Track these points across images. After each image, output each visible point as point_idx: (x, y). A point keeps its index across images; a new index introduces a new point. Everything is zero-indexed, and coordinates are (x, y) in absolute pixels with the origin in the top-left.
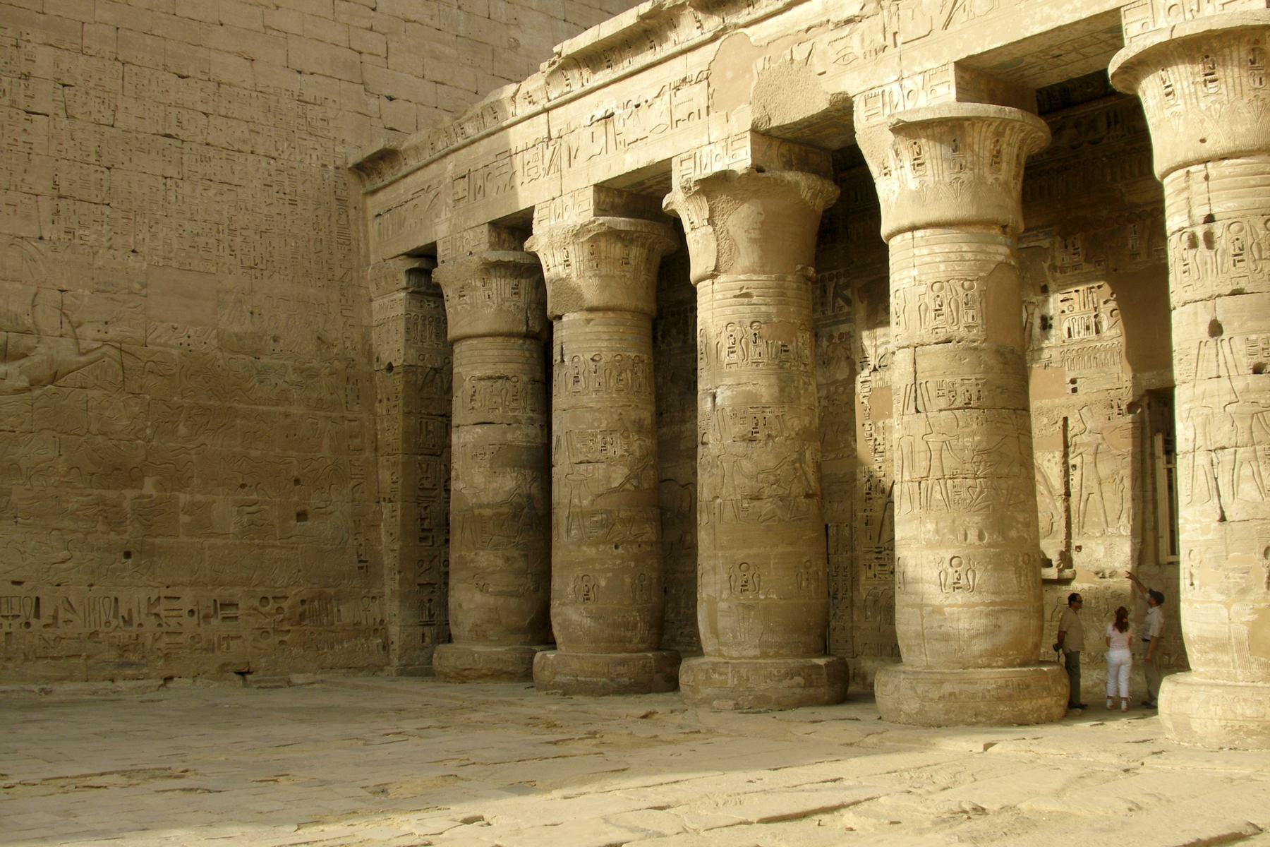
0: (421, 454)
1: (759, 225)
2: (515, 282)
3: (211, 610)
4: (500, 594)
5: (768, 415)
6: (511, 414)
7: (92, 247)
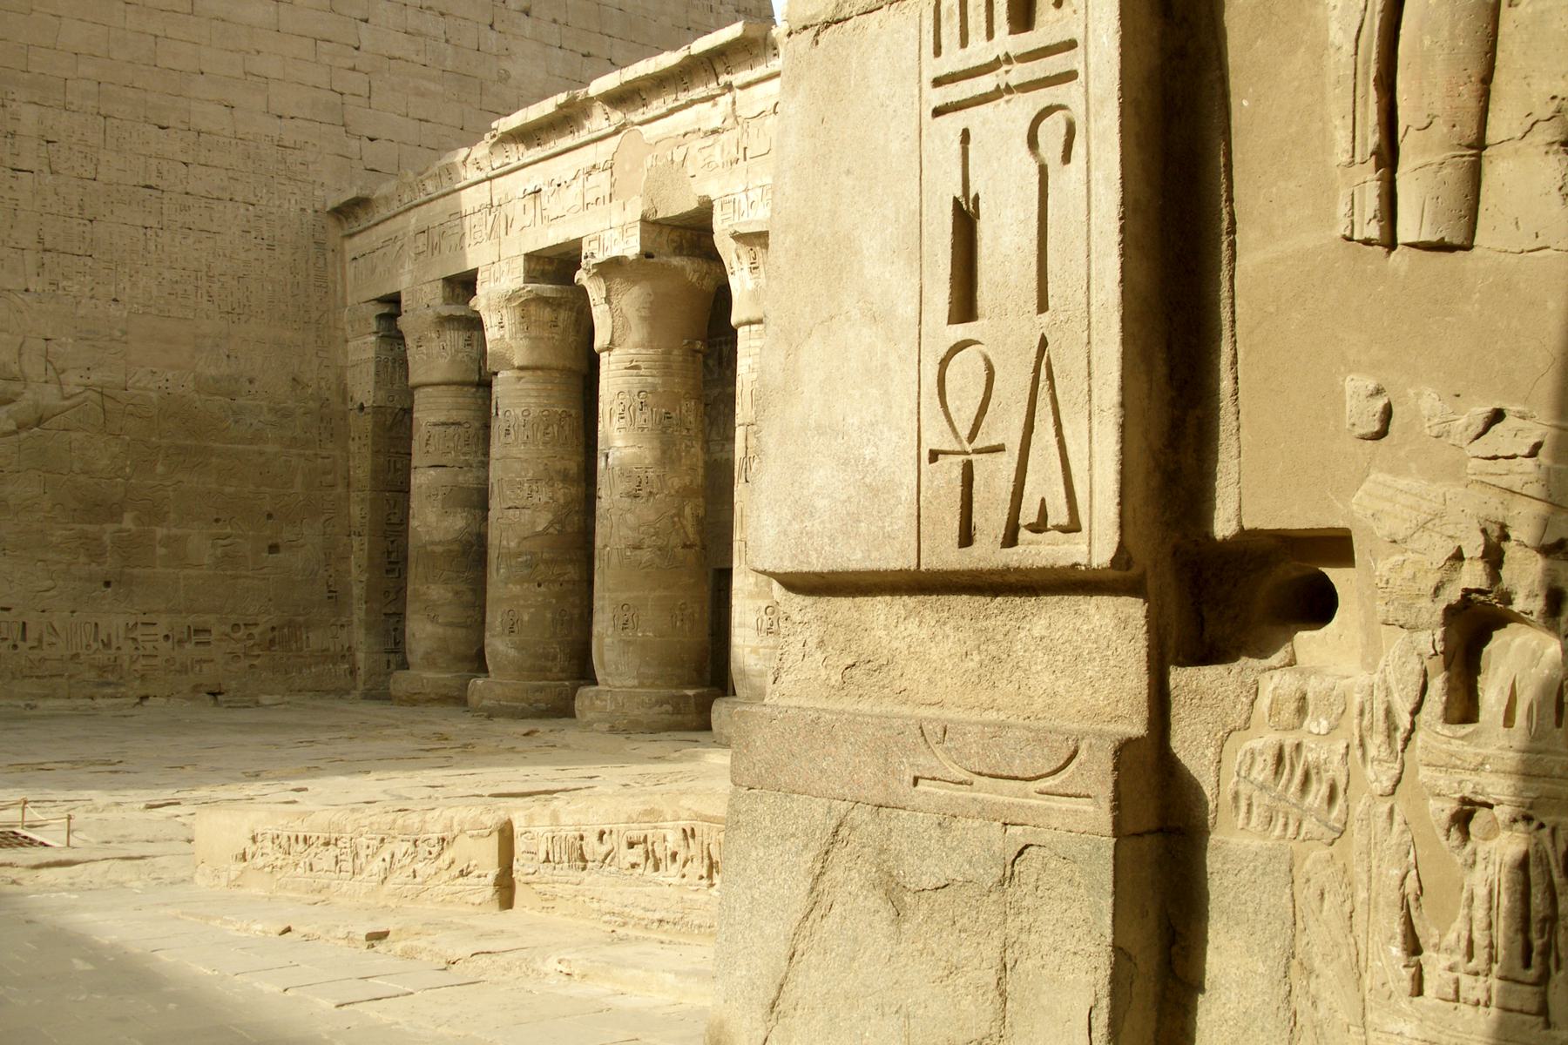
0: (389, 491)
1: (648, 305)
2: (468, 334)
3: (186, 636)
4: (451, 624)
5: (650, 474)
6: (462, 458)
7: (75, 297)
